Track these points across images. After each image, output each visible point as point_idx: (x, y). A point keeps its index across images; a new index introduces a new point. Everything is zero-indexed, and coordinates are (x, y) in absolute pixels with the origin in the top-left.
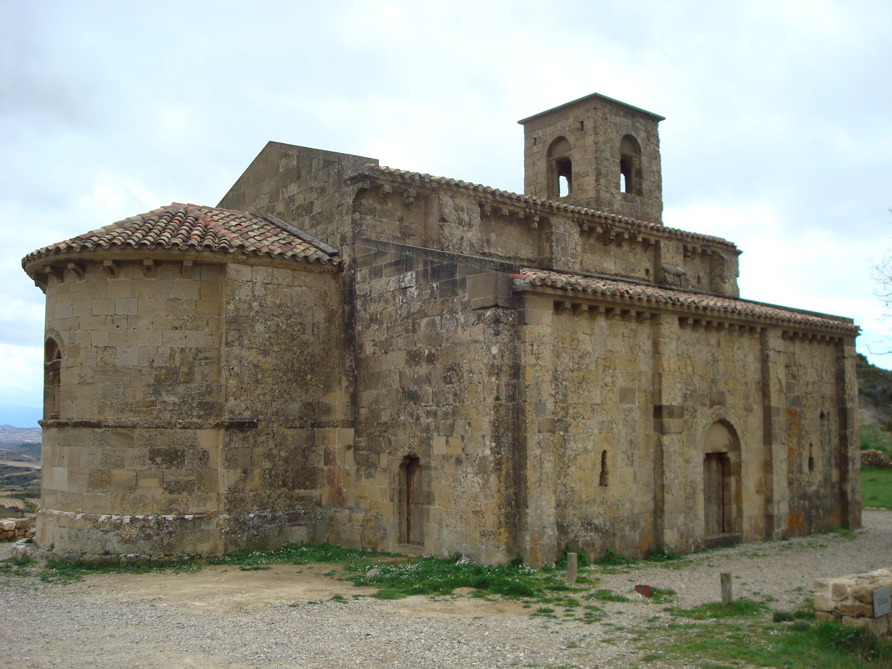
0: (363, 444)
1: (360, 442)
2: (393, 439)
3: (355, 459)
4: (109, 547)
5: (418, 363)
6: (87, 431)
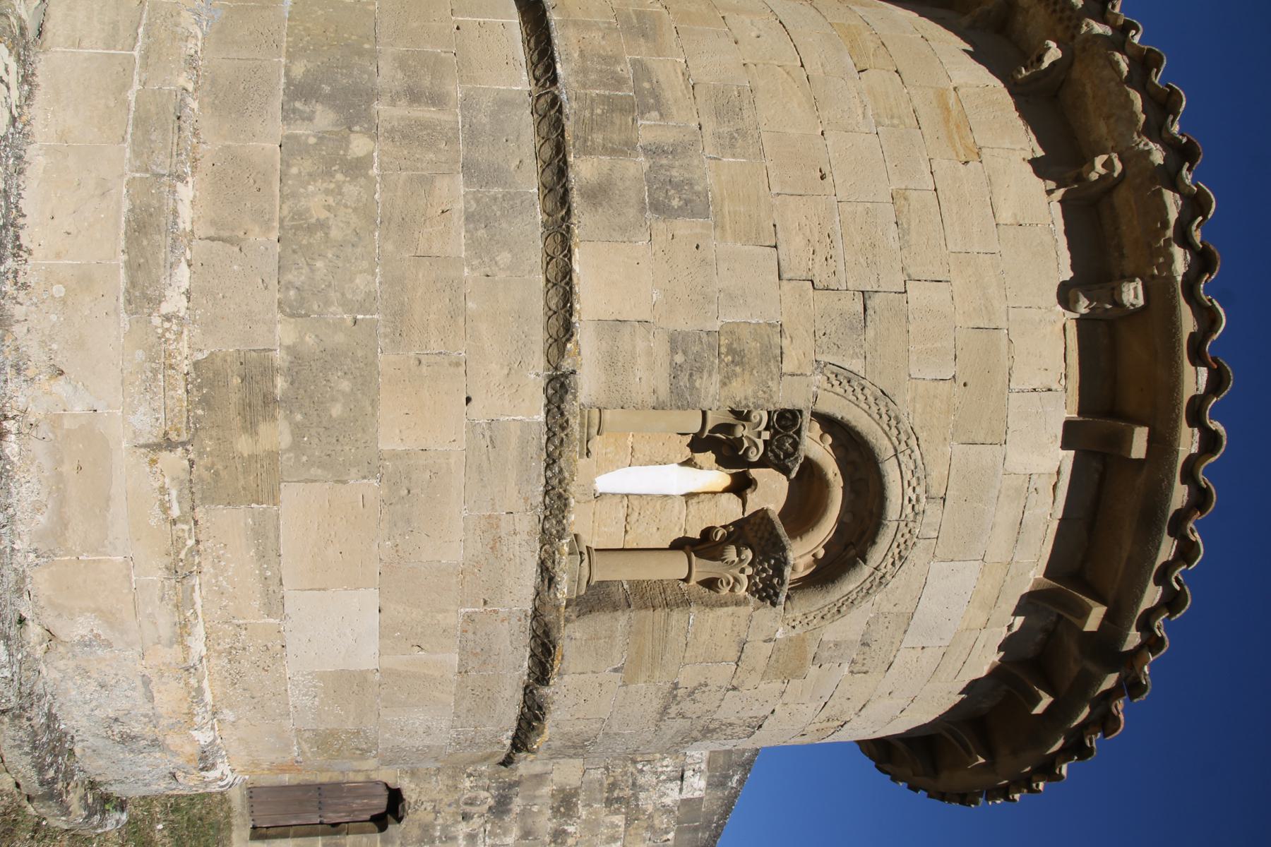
5: (556, 811)
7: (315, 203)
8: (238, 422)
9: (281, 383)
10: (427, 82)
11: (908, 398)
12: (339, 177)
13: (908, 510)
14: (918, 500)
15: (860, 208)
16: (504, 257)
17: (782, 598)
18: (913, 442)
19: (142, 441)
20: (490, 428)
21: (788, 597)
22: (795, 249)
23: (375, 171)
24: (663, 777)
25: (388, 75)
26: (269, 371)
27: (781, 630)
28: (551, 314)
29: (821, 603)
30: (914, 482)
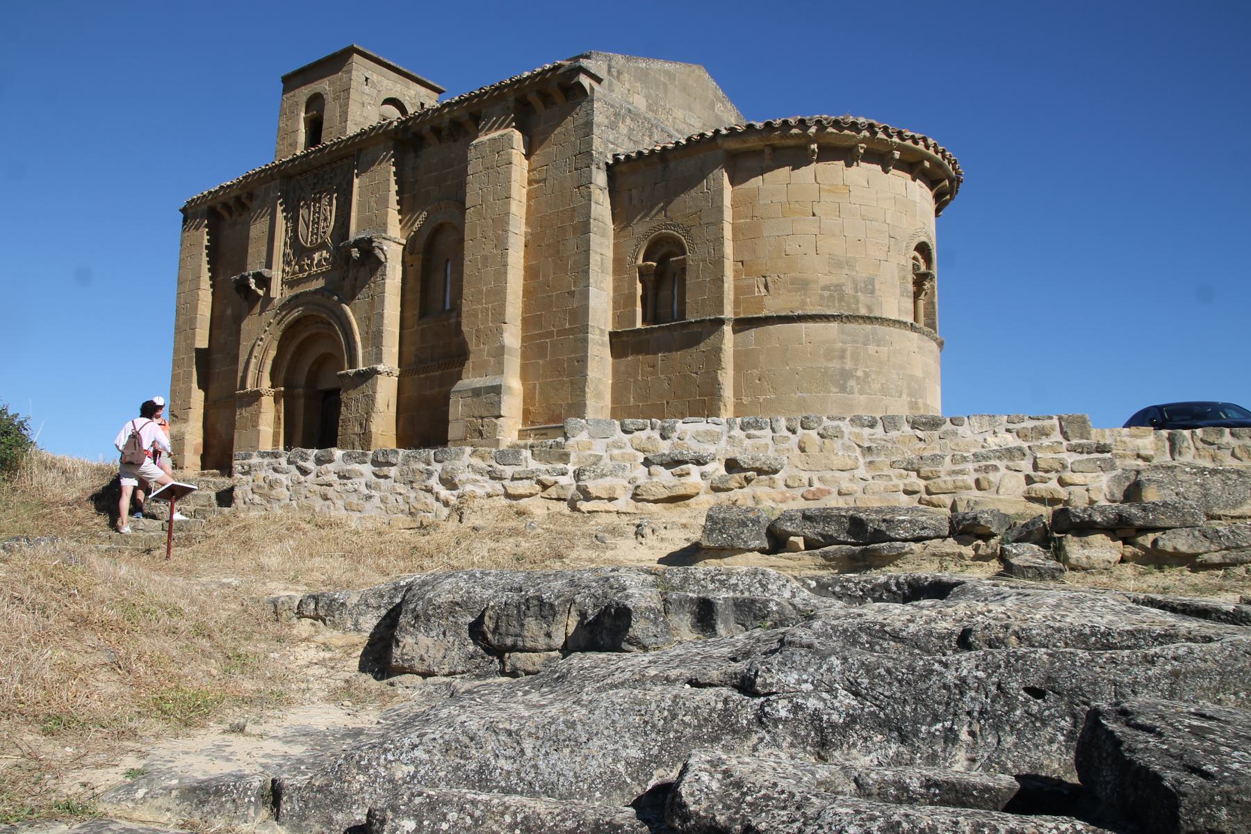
7: (877, 386)
22: (882, 256)
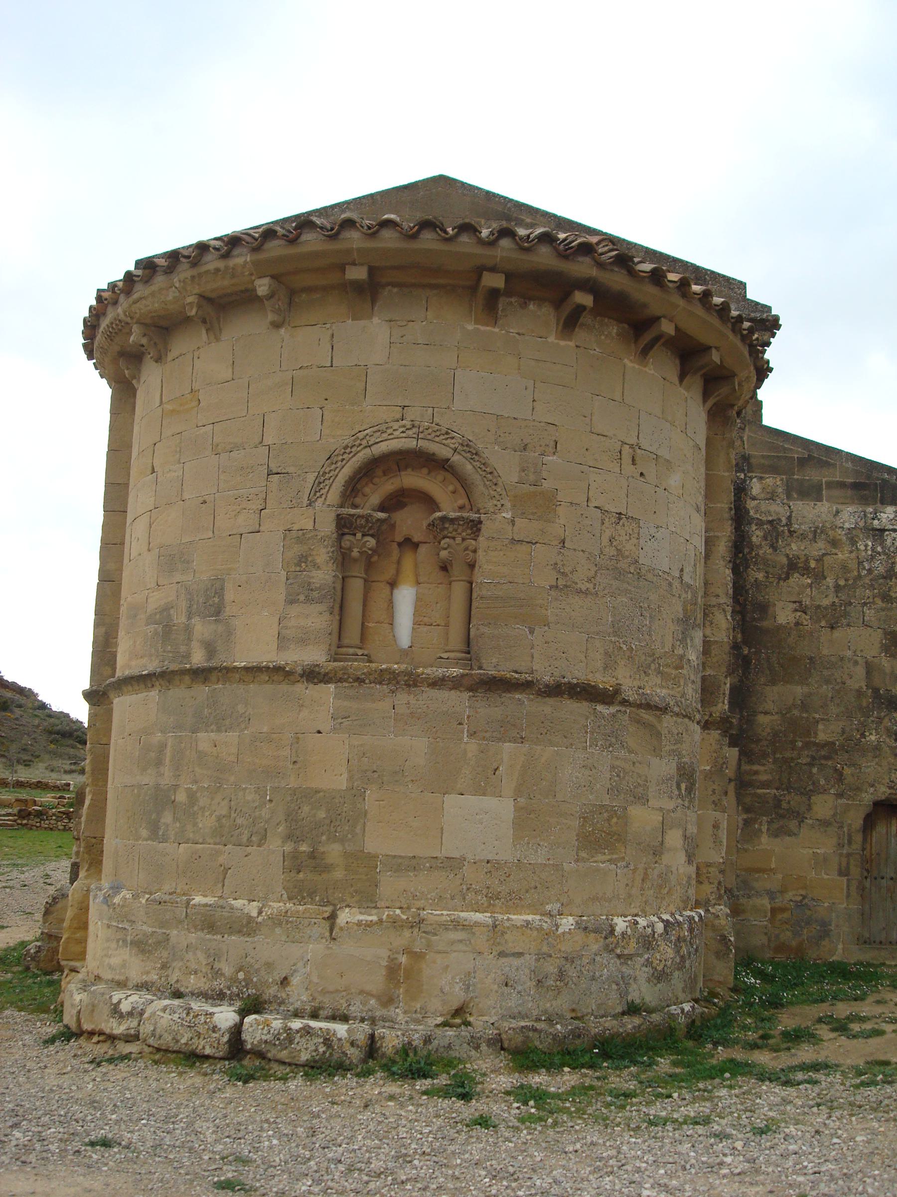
0: (764, 777)
1: (756, 773)
2: (847, 771)
3: (739, 801)
4: (634, 996)
6: (573, 710)
7: (206, 823)
8: (324, 876)
9: (304, 848)
10: (153, 755)
11: (332, 441)
12: (196, 808)
13: (410, 433)
14: (404, 426)
15: (222, 477)
16: (241, 708)
17: (475, 516)
18: (361, 435)
19: (327, 934)
20: (337, 719)
21: (478, 512)
23: (194, 787)
24: (879, 549)
25: (148, 779)
26: (295, 855)
27: (504, 515)
28: (271, 681)
29: (481, 488)
30: (389, 431)
